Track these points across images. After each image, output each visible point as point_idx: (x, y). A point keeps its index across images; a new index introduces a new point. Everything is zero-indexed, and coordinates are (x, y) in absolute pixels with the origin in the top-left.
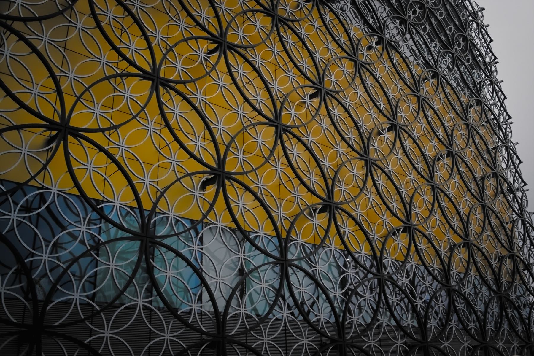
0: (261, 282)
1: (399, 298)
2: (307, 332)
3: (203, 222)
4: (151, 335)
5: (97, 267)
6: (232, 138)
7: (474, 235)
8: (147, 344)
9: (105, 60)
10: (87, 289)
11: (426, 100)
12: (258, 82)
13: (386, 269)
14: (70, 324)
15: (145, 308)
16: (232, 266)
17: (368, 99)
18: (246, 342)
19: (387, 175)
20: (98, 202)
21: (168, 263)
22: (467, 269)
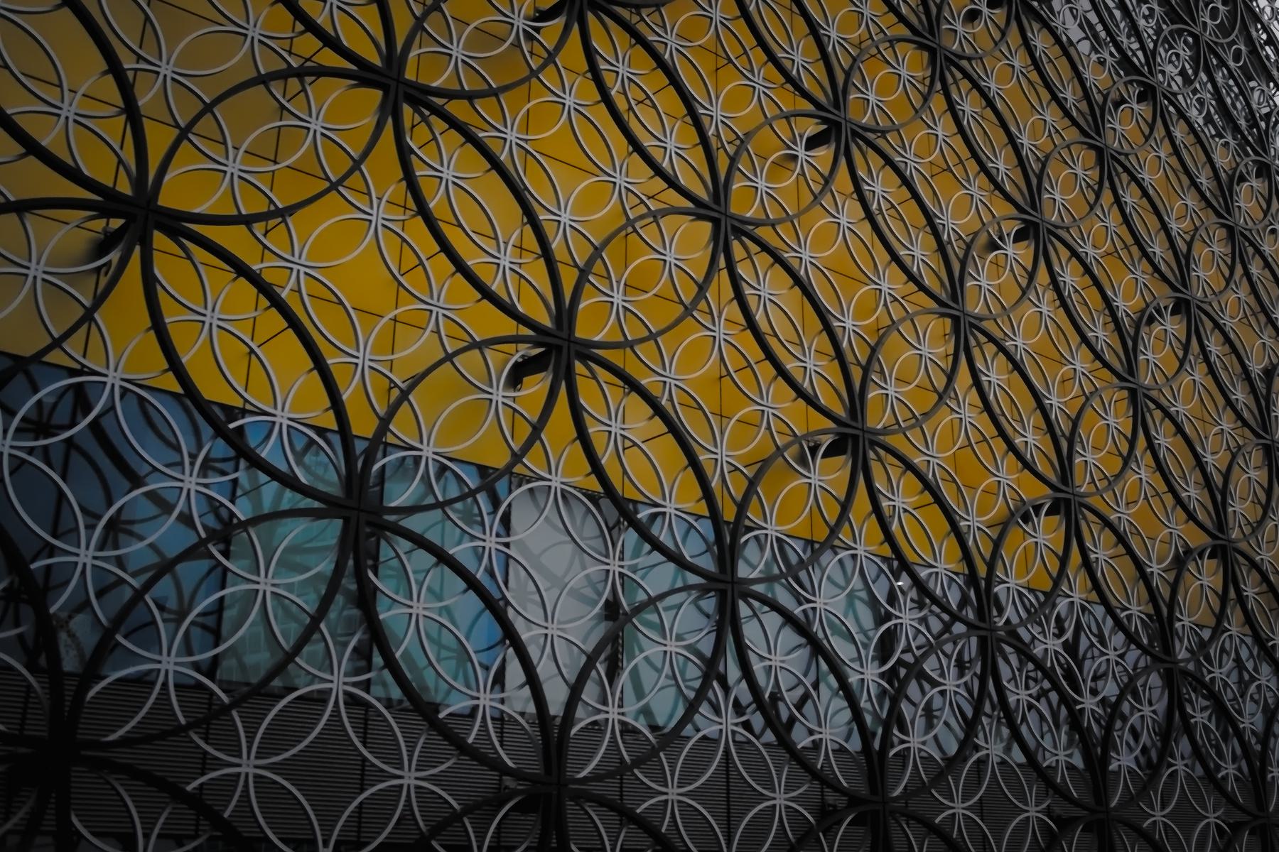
0: (664, 637)
1: (1034, 691)
2: (784, 776)
3: (512, 473)
4: (365, 773)
5: (223, 587)
6: (596, 248)
7: (1240, 526)
8: (355, 798)
9: (258, 30)
10: (195, 645)
11: (1122, 158)
12: (669, 101)
13: (1001, 611)
14: (148, 739)
15: (352, 700)
16: (589, 592)
17: (964, 153)
18: (621, 799)
19: (1010, 358)
20: (232, 412)
21: (416, 581)
22: (1220, 616)
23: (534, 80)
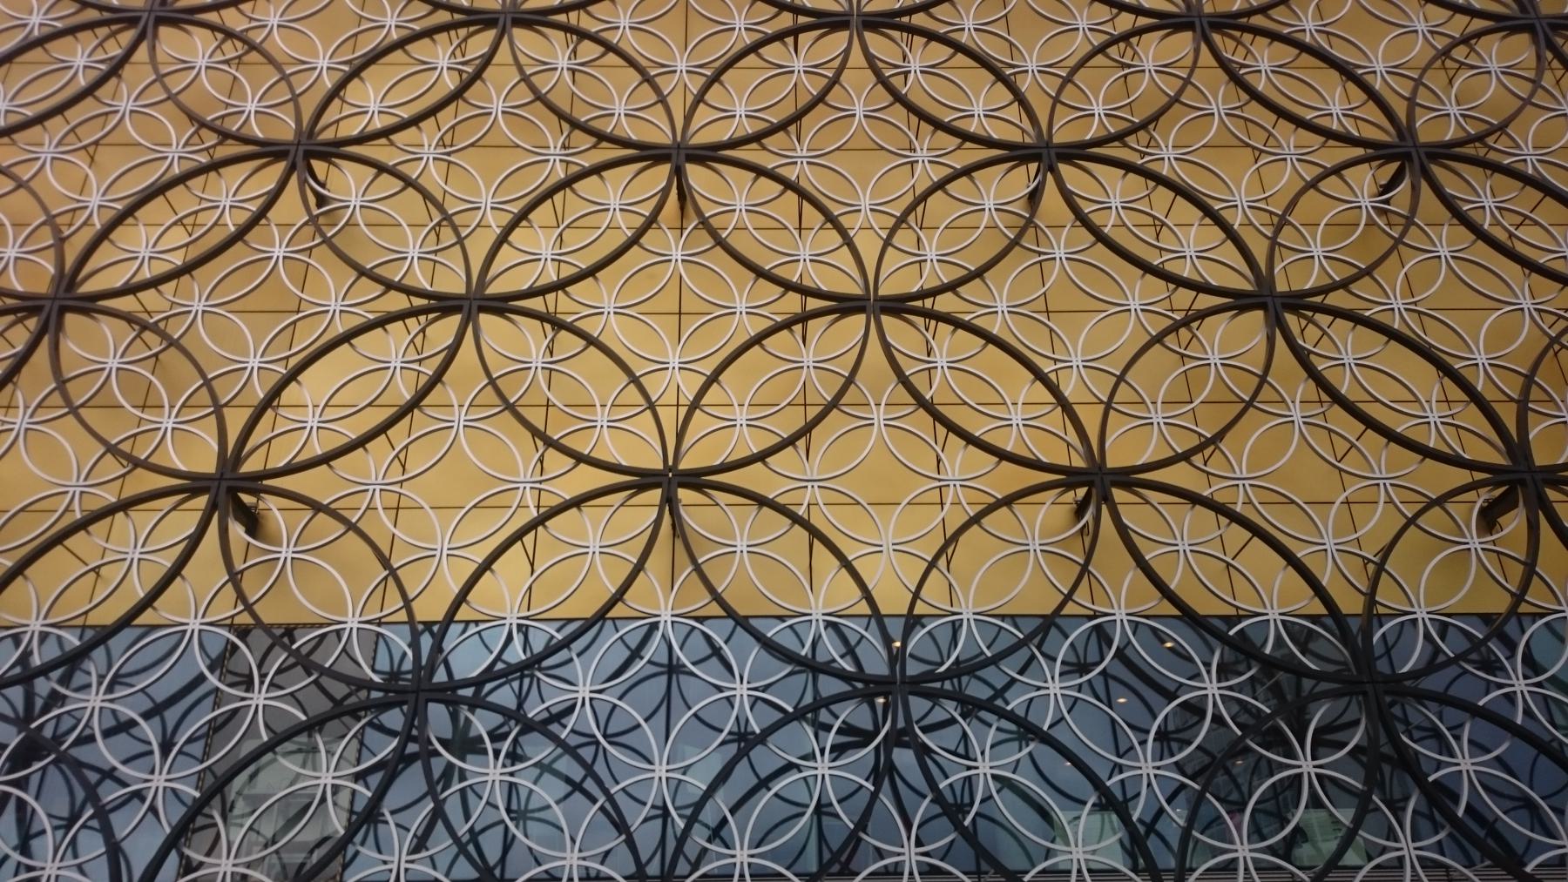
23: (1401, 247)
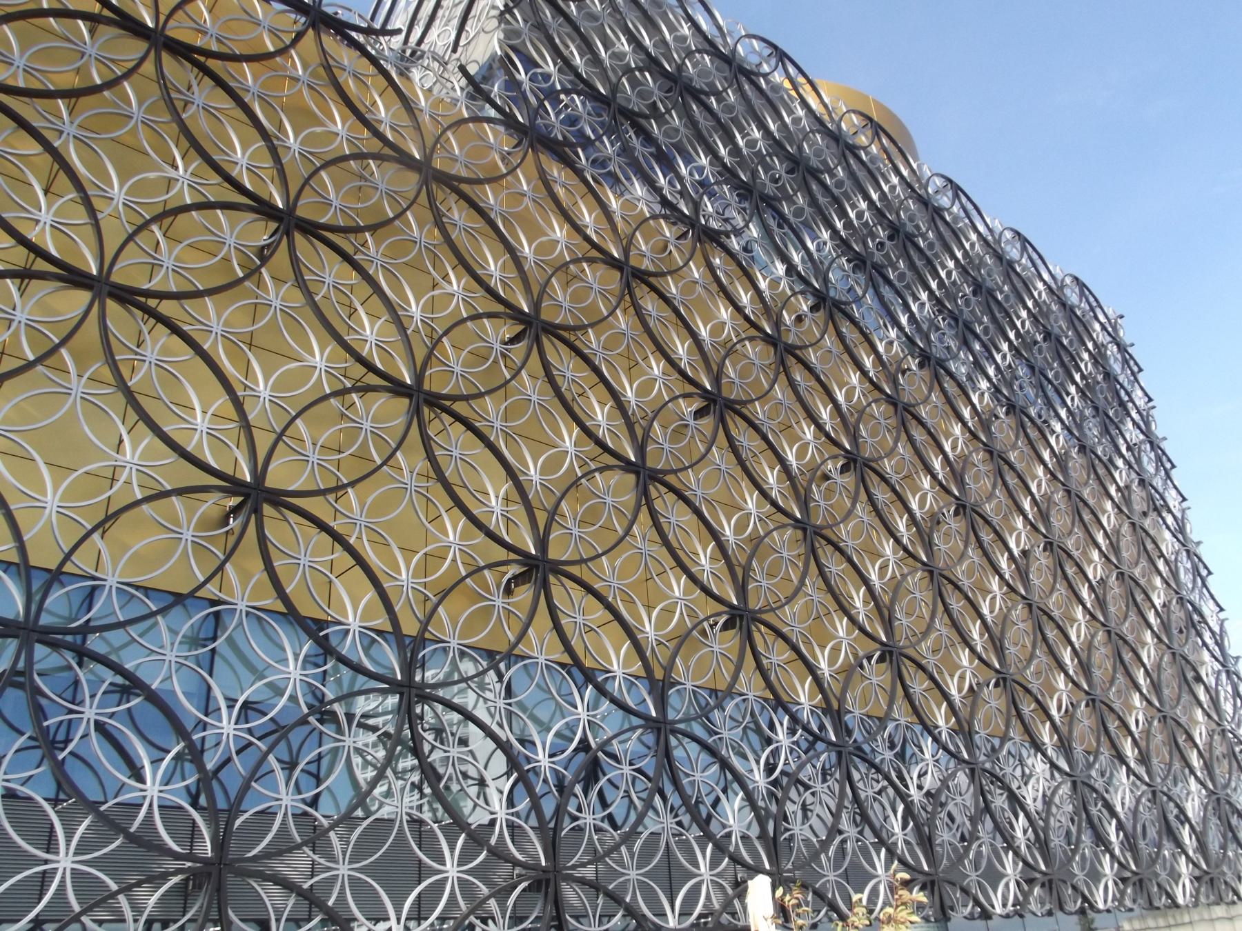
5: (320, 746)
10: (302, 786)
20: (321, 624)
